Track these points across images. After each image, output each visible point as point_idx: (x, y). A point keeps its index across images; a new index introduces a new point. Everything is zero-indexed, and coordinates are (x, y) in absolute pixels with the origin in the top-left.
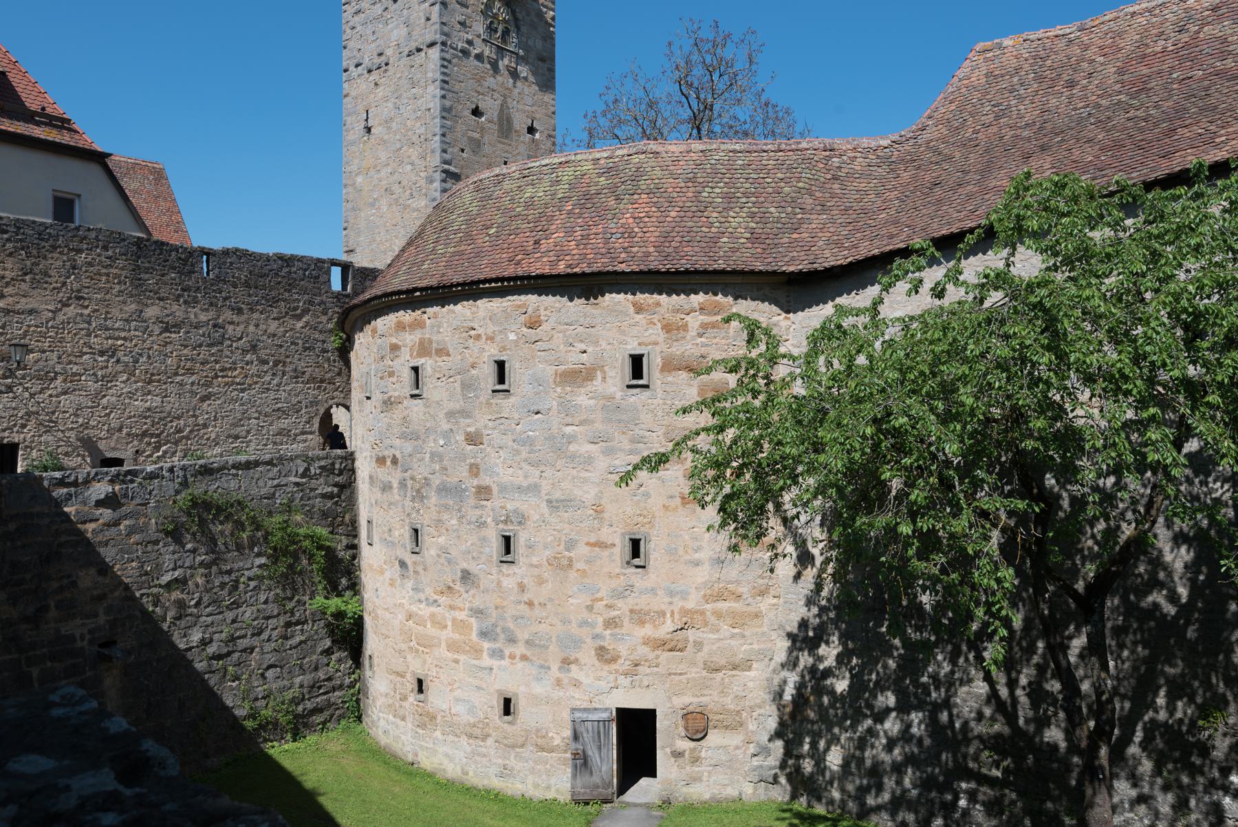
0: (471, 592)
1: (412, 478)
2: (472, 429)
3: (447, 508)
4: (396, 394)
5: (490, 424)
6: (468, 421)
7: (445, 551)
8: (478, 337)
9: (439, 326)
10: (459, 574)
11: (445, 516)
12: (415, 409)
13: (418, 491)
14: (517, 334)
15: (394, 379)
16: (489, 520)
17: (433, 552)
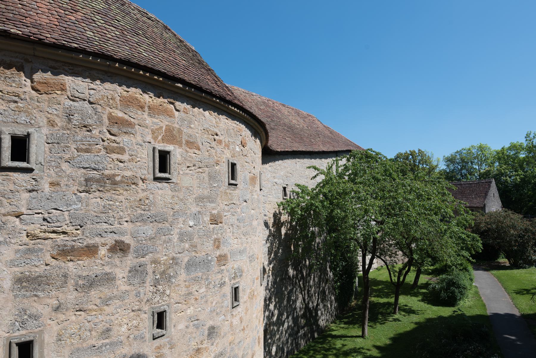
0: (217, 341)
1: (155, 262)
2: (215, 212)
3: (196, 280)
4: (128, 174)
5: (226, 208)
6: (213, 205)
7: (194, 319)
8: (220, 142)
9: (190, 122)
10: (206, 333)
11: (196, 288)
12: (160, 192)
13: (163, 273)
14: (239, 148)
15: (125, 157)
16: (227, 280)
17: (181, 326)
